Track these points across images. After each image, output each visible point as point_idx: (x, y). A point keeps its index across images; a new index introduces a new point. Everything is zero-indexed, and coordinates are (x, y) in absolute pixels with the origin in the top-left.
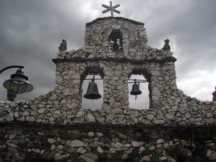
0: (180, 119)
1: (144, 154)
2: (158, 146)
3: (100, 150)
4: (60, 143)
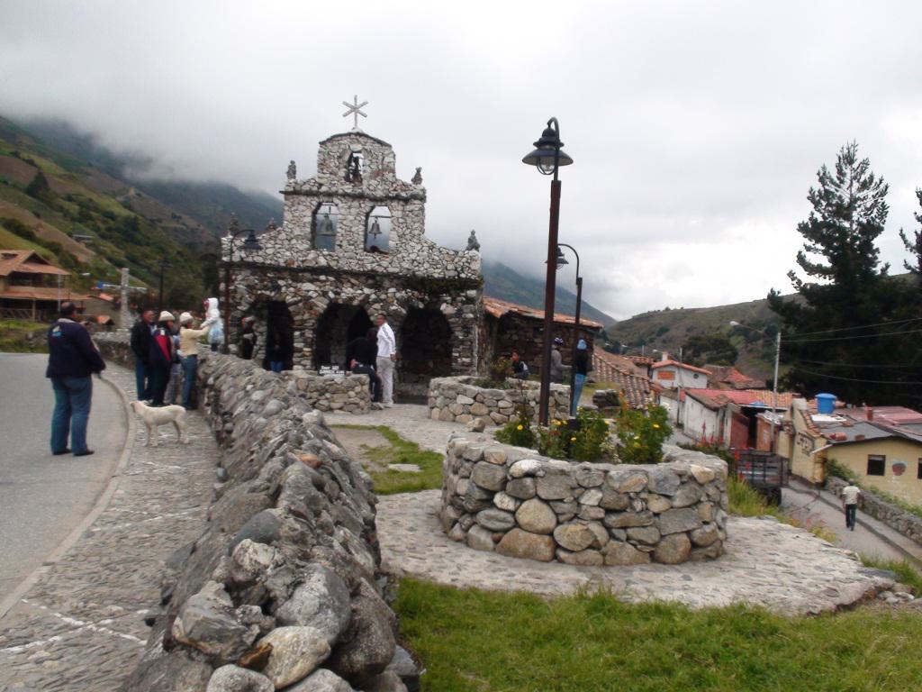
0: (417, 268)
1: (375, 301)
2: (389, 295)
3: (331, 295)
4: (290, 286)
